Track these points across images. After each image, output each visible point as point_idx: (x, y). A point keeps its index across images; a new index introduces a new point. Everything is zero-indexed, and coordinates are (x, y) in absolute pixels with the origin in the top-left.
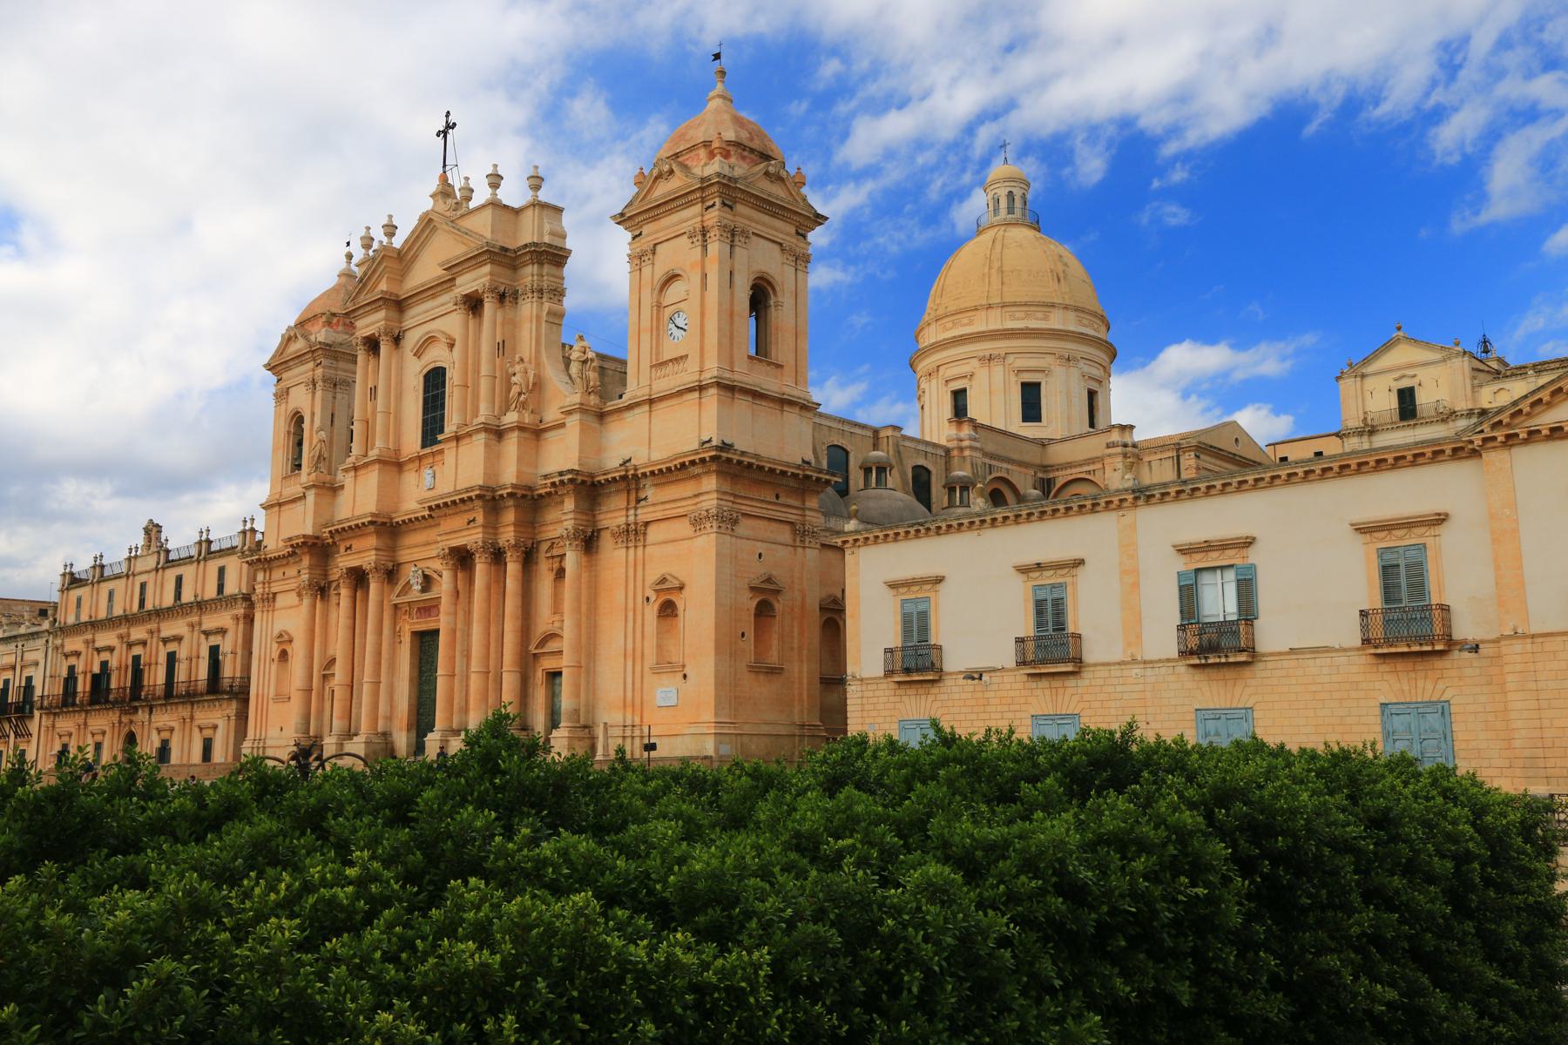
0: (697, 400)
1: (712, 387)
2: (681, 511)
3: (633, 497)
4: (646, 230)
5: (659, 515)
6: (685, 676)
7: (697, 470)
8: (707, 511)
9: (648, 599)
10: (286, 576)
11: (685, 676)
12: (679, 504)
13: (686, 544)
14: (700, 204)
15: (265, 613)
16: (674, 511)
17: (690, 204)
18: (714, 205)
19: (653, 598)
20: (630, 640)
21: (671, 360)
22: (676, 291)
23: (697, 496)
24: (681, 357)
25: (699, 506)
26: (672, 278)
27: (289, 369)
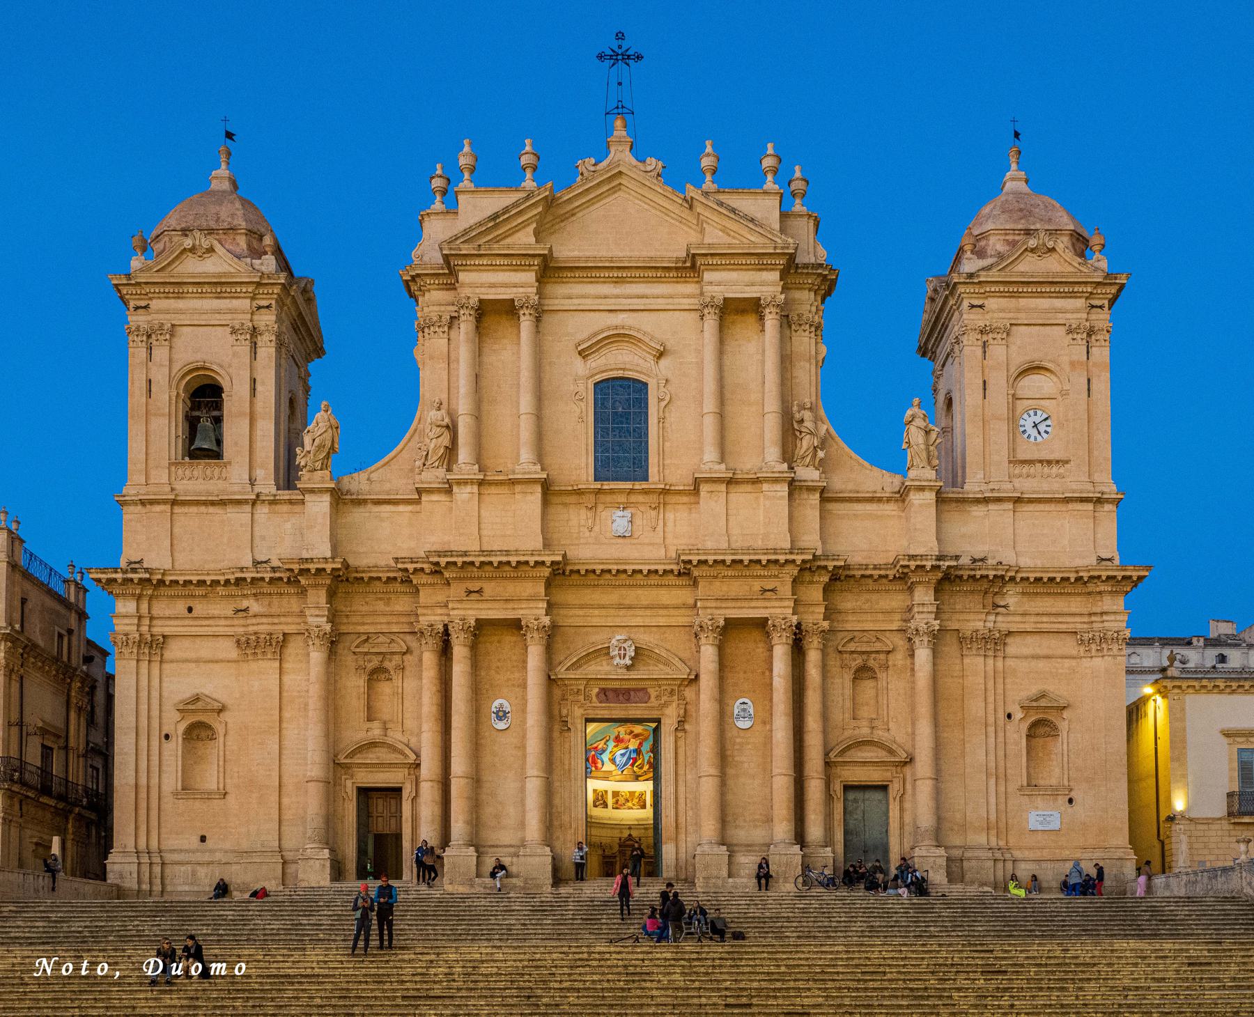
0: (1091, 513)
1: (1111, 503)
2: (1071, 627)
3: (989, 600)
4: (992, 303)
5: (1029, 627)
6: (1071, 801)
7: (1103, 587)
8: (1117, 632)
9: (1009, 716)
10: (195, 613)
11: (1071, 801)
12: (1060, 620)
13: (1067, 663)
14: (1084, 300)
15: (144, 665)
16: (1057, 626)
17: (1073, 295)
18: (1101, 307)
19: (1018, 715)
20: (992, 757)
21: (1041, 462)
22: (1035, 384)
23: (1090, 614)
24: (1058, 462)
25: (1106, 624)
26: (1034, 368)
27: (179, 296)
